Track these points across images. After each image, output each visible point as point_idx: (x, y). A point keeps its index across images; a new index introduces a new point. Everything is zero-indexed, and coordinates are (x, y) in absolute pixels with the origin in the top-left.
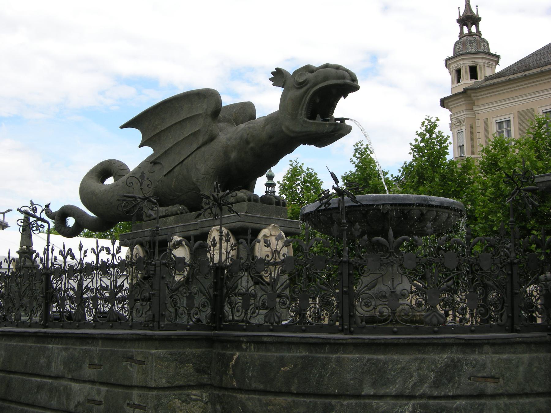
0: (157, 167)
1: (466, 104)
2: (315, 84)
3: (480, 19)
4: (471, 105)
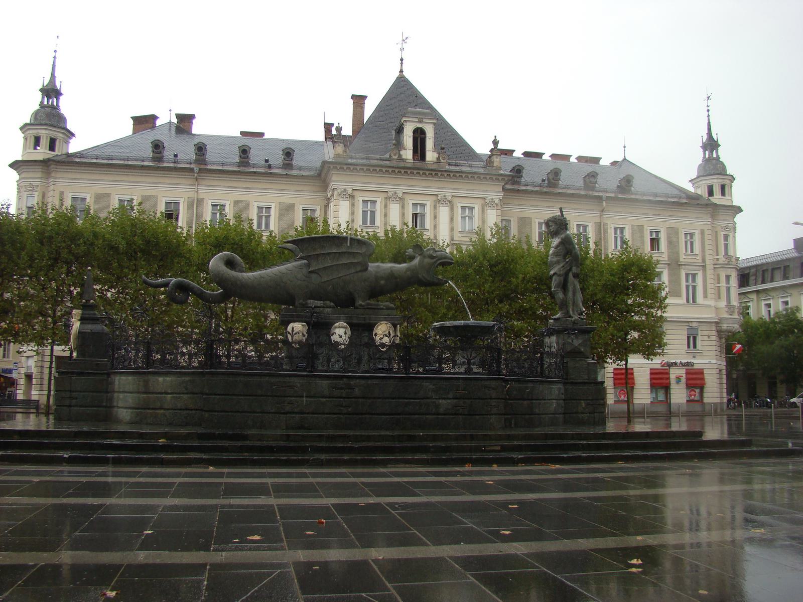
0: (314, 276)
1: (42, 171)
2: (439, 260)
3: (61, 94)
4: (47, 175)
